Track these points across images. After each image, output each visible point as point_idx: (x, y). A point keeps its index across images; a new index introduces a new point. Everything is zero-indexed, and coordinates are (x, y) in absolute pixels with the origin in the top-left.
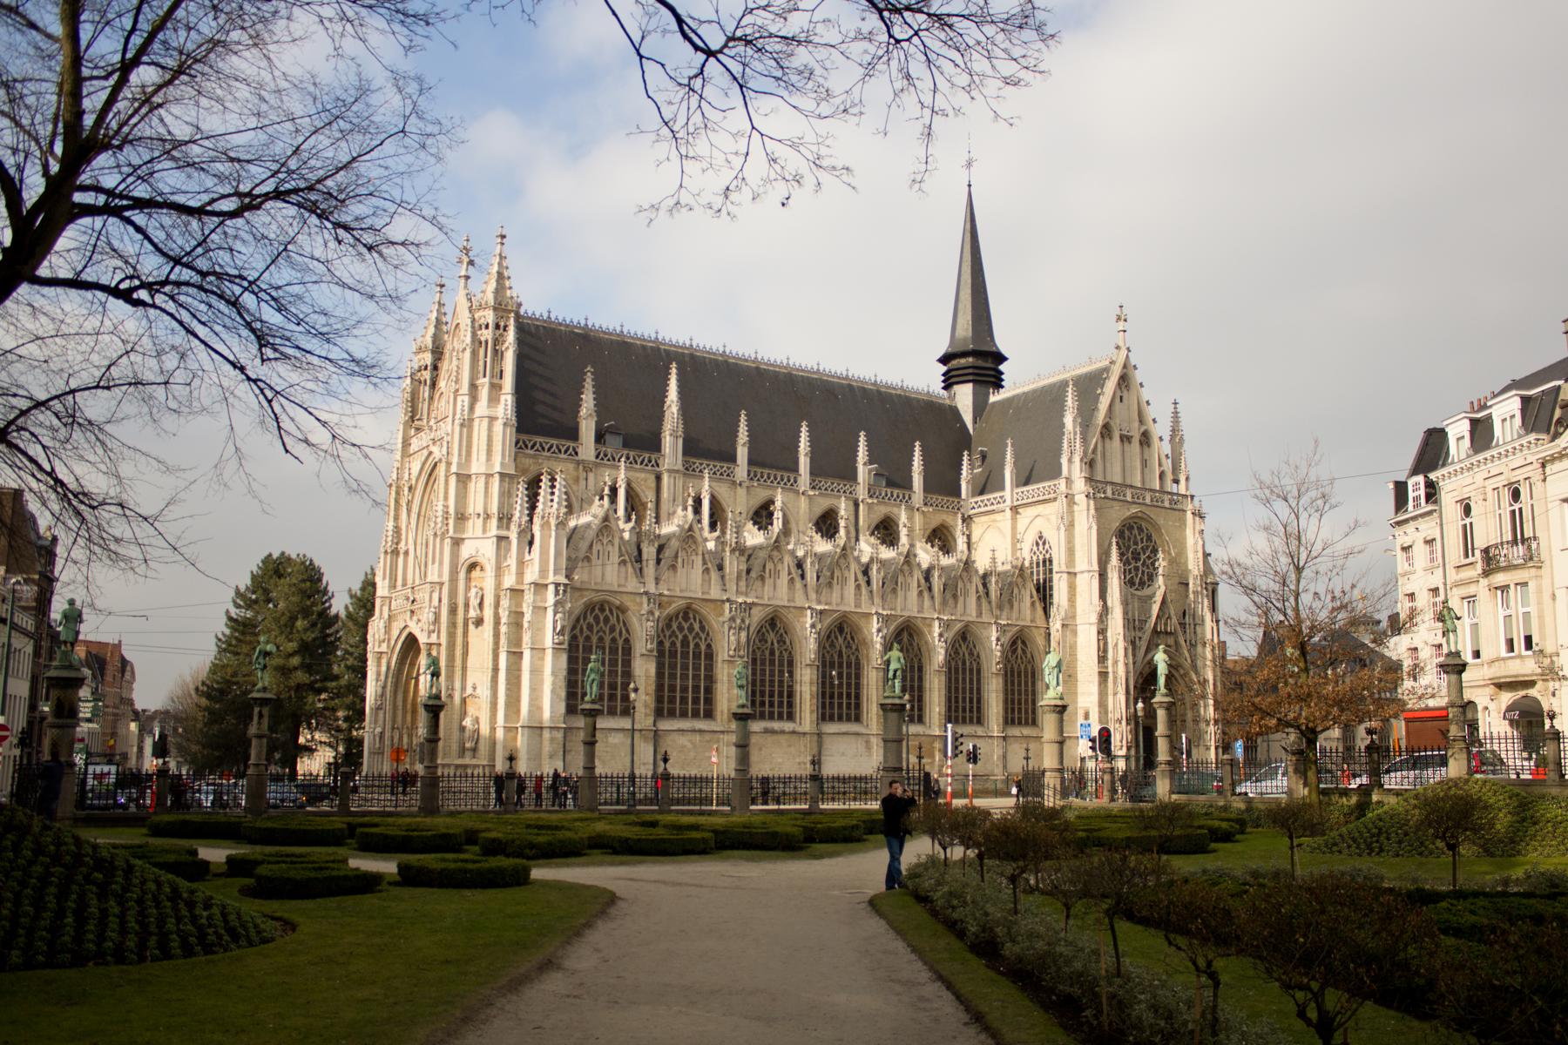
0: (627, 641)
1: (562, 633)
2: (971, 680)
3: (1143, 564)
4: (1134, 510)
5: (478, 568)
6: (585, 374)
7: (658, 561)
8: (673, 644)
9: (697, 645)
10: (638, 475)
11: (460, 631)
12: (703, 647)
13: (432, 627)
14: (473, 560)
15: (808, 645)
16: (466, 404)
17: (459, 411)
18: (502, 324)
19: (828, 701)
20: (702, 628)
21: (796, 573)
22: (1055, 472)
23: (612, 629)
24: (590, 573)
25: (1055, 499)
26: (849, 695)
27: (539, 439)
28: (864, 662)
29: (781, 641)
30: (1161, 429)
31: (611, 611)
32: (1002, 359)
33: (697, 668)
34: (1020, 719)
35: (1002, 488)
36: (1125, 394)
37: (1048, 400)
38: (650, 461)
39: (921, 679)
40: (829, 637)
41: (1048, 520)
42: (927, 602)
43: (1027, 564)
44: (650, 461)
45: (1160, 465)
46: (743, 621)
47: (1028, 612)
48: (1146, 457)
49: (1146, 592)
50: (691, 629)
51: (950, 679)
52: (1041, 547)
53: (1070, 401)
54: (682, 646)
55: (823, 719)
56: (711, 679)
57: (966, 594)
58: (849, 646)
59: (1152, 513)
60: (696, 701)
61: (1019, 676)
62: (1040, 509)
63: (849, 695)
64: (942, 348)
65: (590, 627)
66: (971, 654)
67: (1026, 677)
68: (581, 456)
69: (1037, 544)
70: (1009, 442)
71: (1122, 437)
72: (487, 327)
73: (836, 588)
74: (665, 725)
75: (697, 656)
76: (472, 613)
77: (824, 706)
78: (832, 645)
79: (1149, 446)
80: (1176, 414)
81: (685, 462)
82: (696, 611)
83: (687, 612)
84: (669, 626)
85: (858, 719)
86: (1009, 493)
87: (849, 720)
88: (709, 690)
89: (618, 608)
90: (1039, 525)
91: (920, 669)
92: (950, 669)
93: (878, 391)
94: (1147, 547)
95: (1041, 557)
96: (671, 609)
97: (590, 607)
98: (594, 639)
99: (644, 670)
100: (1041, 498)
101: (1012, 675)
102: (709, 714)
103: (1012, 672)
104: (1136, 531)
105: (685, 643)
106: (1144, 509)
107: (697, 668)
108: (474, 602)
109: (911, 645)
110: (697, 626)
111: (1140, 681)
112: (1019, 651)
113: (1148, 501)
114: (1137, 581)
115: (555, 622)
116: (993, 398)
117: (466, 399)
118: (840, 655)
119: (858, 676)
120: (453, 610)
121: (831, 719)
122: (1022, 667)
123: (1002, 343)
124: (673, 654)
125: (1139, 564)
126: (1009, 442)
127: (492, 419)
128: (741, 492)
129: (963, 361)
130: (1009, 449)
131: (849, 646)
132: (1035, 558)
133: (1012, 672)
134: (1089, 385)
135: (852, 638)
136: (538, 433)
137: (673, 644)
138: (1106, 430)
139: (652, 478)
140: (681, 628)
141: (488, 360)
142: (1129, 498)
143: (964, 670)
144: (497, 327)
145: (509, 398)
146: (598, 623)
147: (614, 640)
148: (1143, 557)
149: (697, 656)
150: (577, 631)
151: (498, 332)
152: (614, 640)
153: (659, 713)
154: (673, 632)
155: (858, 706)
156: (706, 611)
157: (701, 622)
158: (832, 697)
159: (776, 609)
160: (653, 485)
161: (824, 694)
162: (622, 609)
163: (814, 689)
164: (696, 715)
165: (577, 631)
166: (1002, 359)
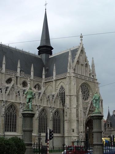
2: (45, 121)
19: (7, 126)
26: (13, 125)
30: (90, 64)
32: (53, 49)
34: (56, 132)
36: (82, 55)
37: (65, 56)
40: (8, 108)
45: (90, 72)
48: (86, 70)
49: (87, 101)
51: (40, 121)
52: (62, 90)
53: (70, 54)
55: (6, 131)
61: (56, 121)
62: (62, 80)
63: (13, 125)
64: (38, 44)
67: (58, 121)
69: (61, 88)
70: (55, 64)
71: (81, 64)
77: (6, 128)
78: (9, 111)
79: (87, 67)
85: (15, 131)
87: (13, 131)
92: (40, 118)
93: (23, 53)
95: (62, 92)
101: (55, 121)
103: (55, 120)
111: (86, 122)
112: (57, 114)
118: (11, 113)
119: (16, 120)
121: (8, 131)
129: (43, 49)
130: (54, 66)
132: (60, 92)
133: (55, 120)
134: (74, 52)
143: (43, 119)
148: (86, 93)
155: (15, 128)
158: (8, 125)
161: (6, 124)
163: (3, 123)
166: (53, 49)
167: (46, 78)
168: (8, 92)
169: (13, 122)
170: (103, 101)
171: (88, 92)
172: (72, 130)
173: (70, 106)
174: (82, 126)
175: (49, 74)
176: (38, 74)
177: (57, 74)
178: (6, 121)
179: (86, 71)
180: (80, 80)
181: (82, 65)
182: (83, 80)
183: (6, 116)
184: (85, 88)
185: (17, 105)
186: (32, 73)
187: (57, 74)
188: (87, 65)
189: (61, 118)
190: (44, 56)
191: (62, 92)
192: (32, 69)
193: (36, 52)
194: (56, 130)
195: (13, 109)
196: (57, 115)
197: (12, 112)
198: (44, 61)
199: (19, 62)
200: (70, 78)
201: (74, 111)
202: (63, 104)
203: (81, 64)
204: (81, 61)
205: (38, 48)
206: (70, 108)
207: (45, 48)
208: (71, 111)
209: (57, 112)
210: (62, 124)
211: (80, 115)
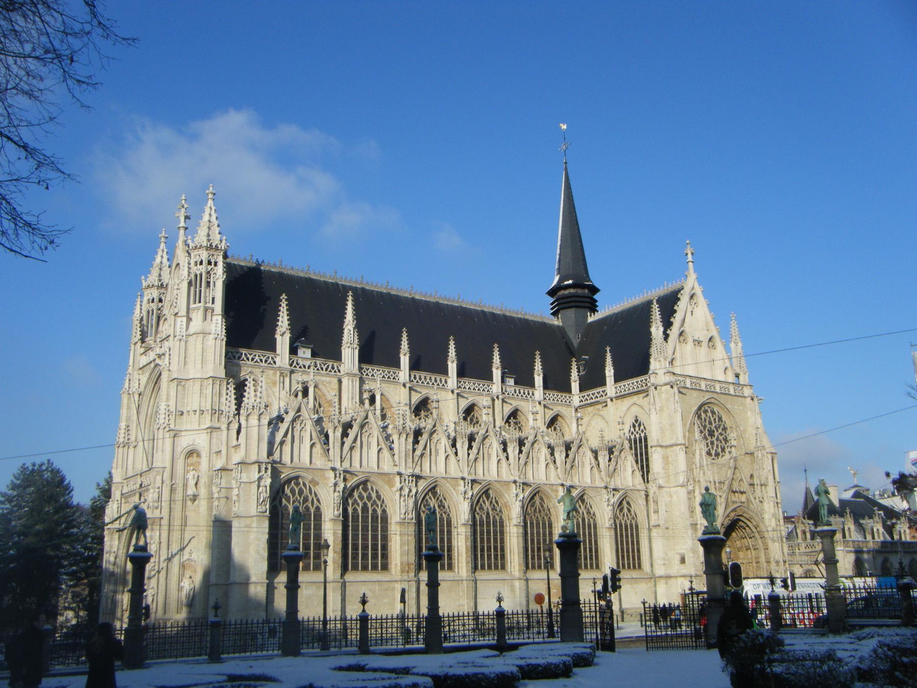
0: (318, 509)
3: (718, 439)
5: (195, 455)
6: (281, 301)
8: (355, 510)
9: (374, 511)
10: (324, 378)
11: (178, 507)
13: (156, 505)
14: (190, 448)
15: (461, 511)
16: (184, 323)
17: (178, 330)
18: (213, 261)
20: (379, 497)
21: (451, 452)
23: (306, 500)
26: (496, 548)
28: (506, 522)
29: (441, 506)
31: (304, 485)
33: (375, 529)
34: (629, 564)
35: (603, 383)
38: (333, 368)
44: (333, 368)
46: (410, 491)
47: (630, 479)
50: (369, 498)
52: (637, 429)
54: (363, 512)
56: (385, 538)
58: (494, 509)
59: (722, 398)
62: (635, 399)
63: (496, 548)
66: (588, 513)
67: (632, 530)
68: (278, 363)
69: (634, 426)
70: (608, 349)
71: (694, 341)
72: (201, 263)
75: (375, 518)
76: (191, 491)
78: (481, 508)
81: (360, 369)
82: (373, 482)
86: (611, 387)
88: (385, 548)
89: (310, 482)
94: (719, 426)
95: (638, 436)
100: (636, 390)
104: (710, 414)
105: (365, 509)
106: (715, 396)
107: (375, 529)
108: (192, 483)
109: (542, 506)
110: (374, 495)
112: (625, 510)
113: (718, 390)
114: (713, 452)
117: (185, 319)
118: (488, 514)
119: (502, 533)
120: (172, 490)
122: (628, 522)
123: (595, 279)
124: (356, 518)
125: (714, 439)
126: (608, 349)
127: (205, 334)
131: (494, 509)
132: (633, 437)
135: (497, 502)
139: (335, 381)
140: (361, 497)
141: (203, 289)
142: (703, 388)
144: (209, 263)
145: (220, 318)
146: (294, 495)
148: (716, 434)
149: (375, 518)
151: (209, 267)
153: (344, 569)
154: (355, 500)
157: (377, 492)
160: (337, 386)
163: (469, 544)
166: (594, 290)
167: (585, 394)
172: (678, 557)
177: (618, 378)
180: (695, 394)
181: (698, 343)
182: (703, 393)
184: (712, 419)
191: (638, 436)
192: (538, 366)
194: (628, 559)
195: (491, 502)
196: (625, 510)
197: (490, 509)
202: (643, 476)
203: (694, 341)
209: (624, 503)
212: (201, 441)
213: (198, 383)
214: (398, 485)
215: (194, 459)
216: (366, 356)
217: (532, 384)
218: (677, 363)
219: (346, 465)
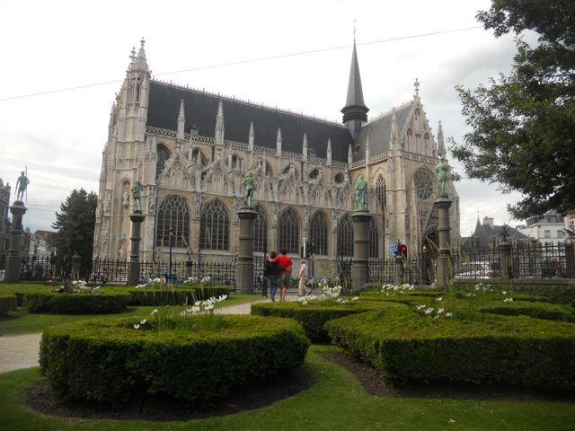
1: (152, 208)
4: (421, 164)
7: (202, 178)
8: (210, 216)
12: (224, 217)
20: (224, 210)
22: (387, 149)
23: (180, 208)
24: (169, 182)
25: (386, 160)
27: (158, 129)
30: (434, 132)
32: (368, 110)
37: (384, 121)
39: (326, 236)
41: (384, 169)
42: (329, 203)
43: (375, 187)
50: (218, 209)
53: (394, 118)
56: (227, 232)
57: (347, 199)
60: (220, 242)
62: (380, 165)
64: (343, 104)
65: (169, 207)
73: (288, 195)
74: (204, 252)
75: (221, 222)
76: (124, 203)
80: (440, 126)
83: (216, 202)
84: (208, 208)
88: (226, 237)
90: (381, 171)
91: (326, 231)
96: (209, 199)
97: (169, 198)
98: (171, 212)
99: (195, 227)
102: (226, 248)
105: (215, 216)
107: (221, 227)
108: (125, 198)
115: (150, 203)
116: (364, 124)
119: (297, 233)
120: (116, 201)
128: (251, 156)
136: (158, 127)
137: (210, 216)
138: (410, 132)
140: (213, 210)
144: (139, 79)
147: (181, 213)
150: (163, 208)
152: (181, 213)
153: (202, 247)
156: (225, 201)
159: (259, 202)
161: (281, 241)
162: (184, 199)
164: (220, 248)
165: (163, 208)
166: (368, 110)
168: (282, 187)
169: (293, 237)
170: (460, 200)
171: (431, 183)
173: (395, 209)
174: (416, 245)
175: (359, 156)
176: (340, 157)
178: (281, 237)
179: (426, 147)
183: (281, 228)
185: (299, 210)
186: (329, 155)
187: (372, 155)
188: (427, 136)
189: (380, 229)
190: (352, 125)
193: (338, 118)
198: (353, 133)
199: (305, 137)
200: (394, 161)
201: (401, 218)
204: (417, 127)
205: (343, 111)
206: (394, 214)
207: (354, 110)
208: (396, 217)
210: (380, 241)
211: (411, 225)
212: (130, 175)
213: (129, 146)
214: (235, 203)
215: (127, 186)
216: (229, 136)
217: (325, 156)
218: (406, 146)
219: (204, 190)
